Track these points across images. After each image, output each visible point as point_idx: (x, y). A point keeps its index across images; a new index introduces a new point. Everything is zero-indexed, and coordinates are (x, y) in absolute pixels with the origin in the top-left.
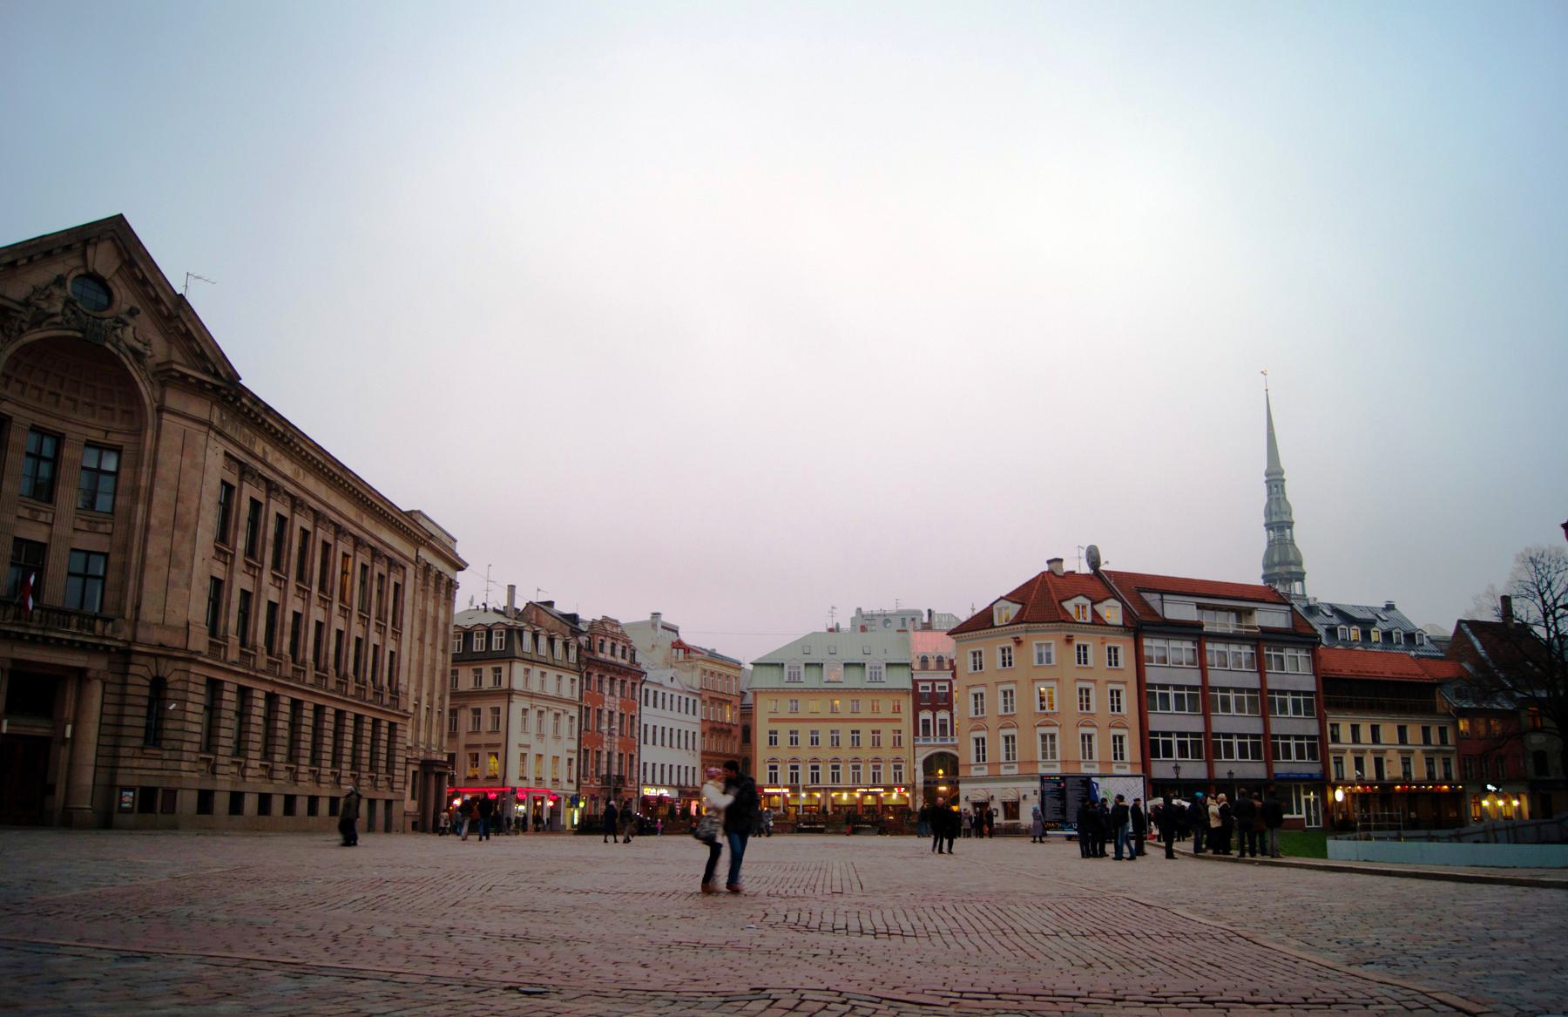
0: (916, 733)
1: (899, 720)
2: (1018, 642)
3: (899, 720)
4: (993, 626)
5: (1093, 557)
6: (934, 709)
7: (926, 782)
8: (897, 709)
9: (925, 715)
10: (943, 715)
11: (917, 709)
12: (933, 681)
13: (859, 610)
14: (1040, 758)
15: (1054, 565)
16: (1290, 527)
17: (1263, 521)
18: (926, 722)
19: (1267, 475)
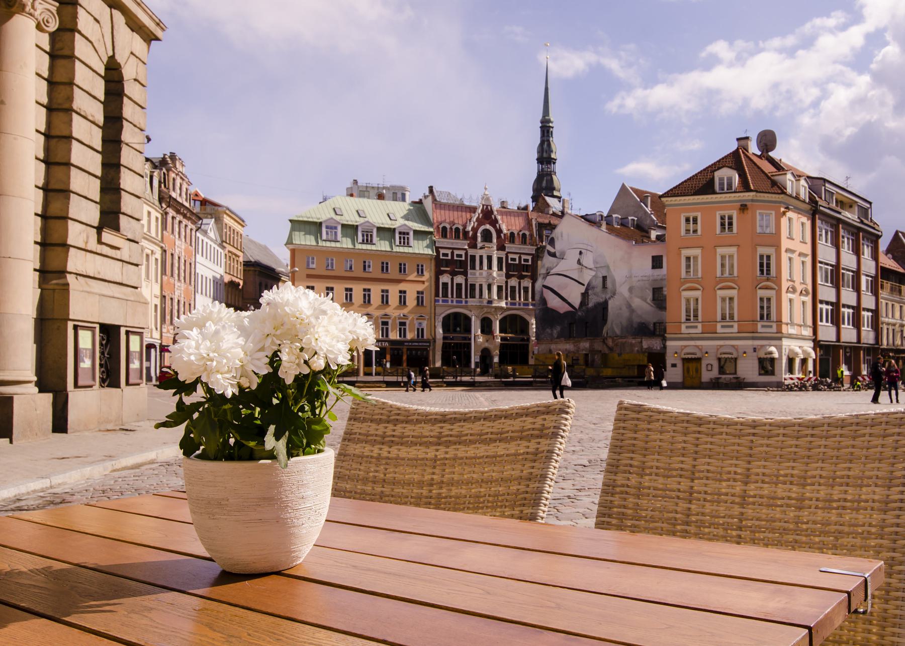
0: (437, 295)
2: (743, 208)
4: (714, 193)
5: (768, 141)
6: (453, 274)
7: (444, 338)
9: (445, 279)
10: (459, 279)
11: (438, 273)
12: (453, 249)
13: (356, 182)
14: (759, 319)
15: (743, 142)
16: (554, 163)
17: (536, 156)
18: (445, 285)
19: (542, 122)
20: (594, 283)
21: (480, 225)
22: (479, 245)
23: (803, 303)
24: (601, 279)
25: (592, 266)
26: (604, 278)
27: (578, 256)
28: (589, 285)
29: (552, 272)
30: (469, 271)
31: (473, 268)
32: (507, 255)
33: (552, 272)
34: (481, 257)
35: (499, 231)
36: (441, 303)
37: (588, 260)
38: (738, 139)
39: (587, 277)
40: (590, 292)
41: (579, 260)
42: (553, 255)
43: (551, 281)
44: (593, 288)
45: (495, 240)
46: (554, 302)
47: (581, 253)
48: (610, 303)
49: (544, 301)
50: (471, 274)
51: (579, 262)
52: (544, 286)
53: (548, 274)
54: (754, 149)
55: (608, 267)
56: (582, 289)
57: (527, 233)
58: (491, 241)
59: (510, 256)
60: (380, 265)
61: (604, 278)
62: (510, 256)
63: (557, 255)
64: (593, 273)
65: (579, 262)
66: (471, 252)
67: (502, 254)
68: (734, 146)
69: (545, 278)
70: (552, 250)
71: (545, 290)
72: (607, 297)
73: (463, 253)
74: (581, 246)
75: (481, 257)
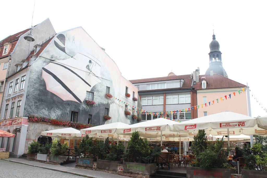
20: (99, 88)
25: (99, 76)
27: (88, 63)
33: (57, 61)
37: (95, 69)
39: (93, 82)
41: (88, 66)
43: (51, 67)
44: (98, 91)
46: (53, 87)
47: (90, 62)
48: (111, 106)
49: (43, 84)
51: (88, 67)
52: (43, 69)
53: (52, 61)
55: (112, 82)
56: (89, 89)
61: (108, 88)
64: (100, 81)
65: (88, 67)
71: (44, 73)
72: (110, 102)
74: (92, 58)
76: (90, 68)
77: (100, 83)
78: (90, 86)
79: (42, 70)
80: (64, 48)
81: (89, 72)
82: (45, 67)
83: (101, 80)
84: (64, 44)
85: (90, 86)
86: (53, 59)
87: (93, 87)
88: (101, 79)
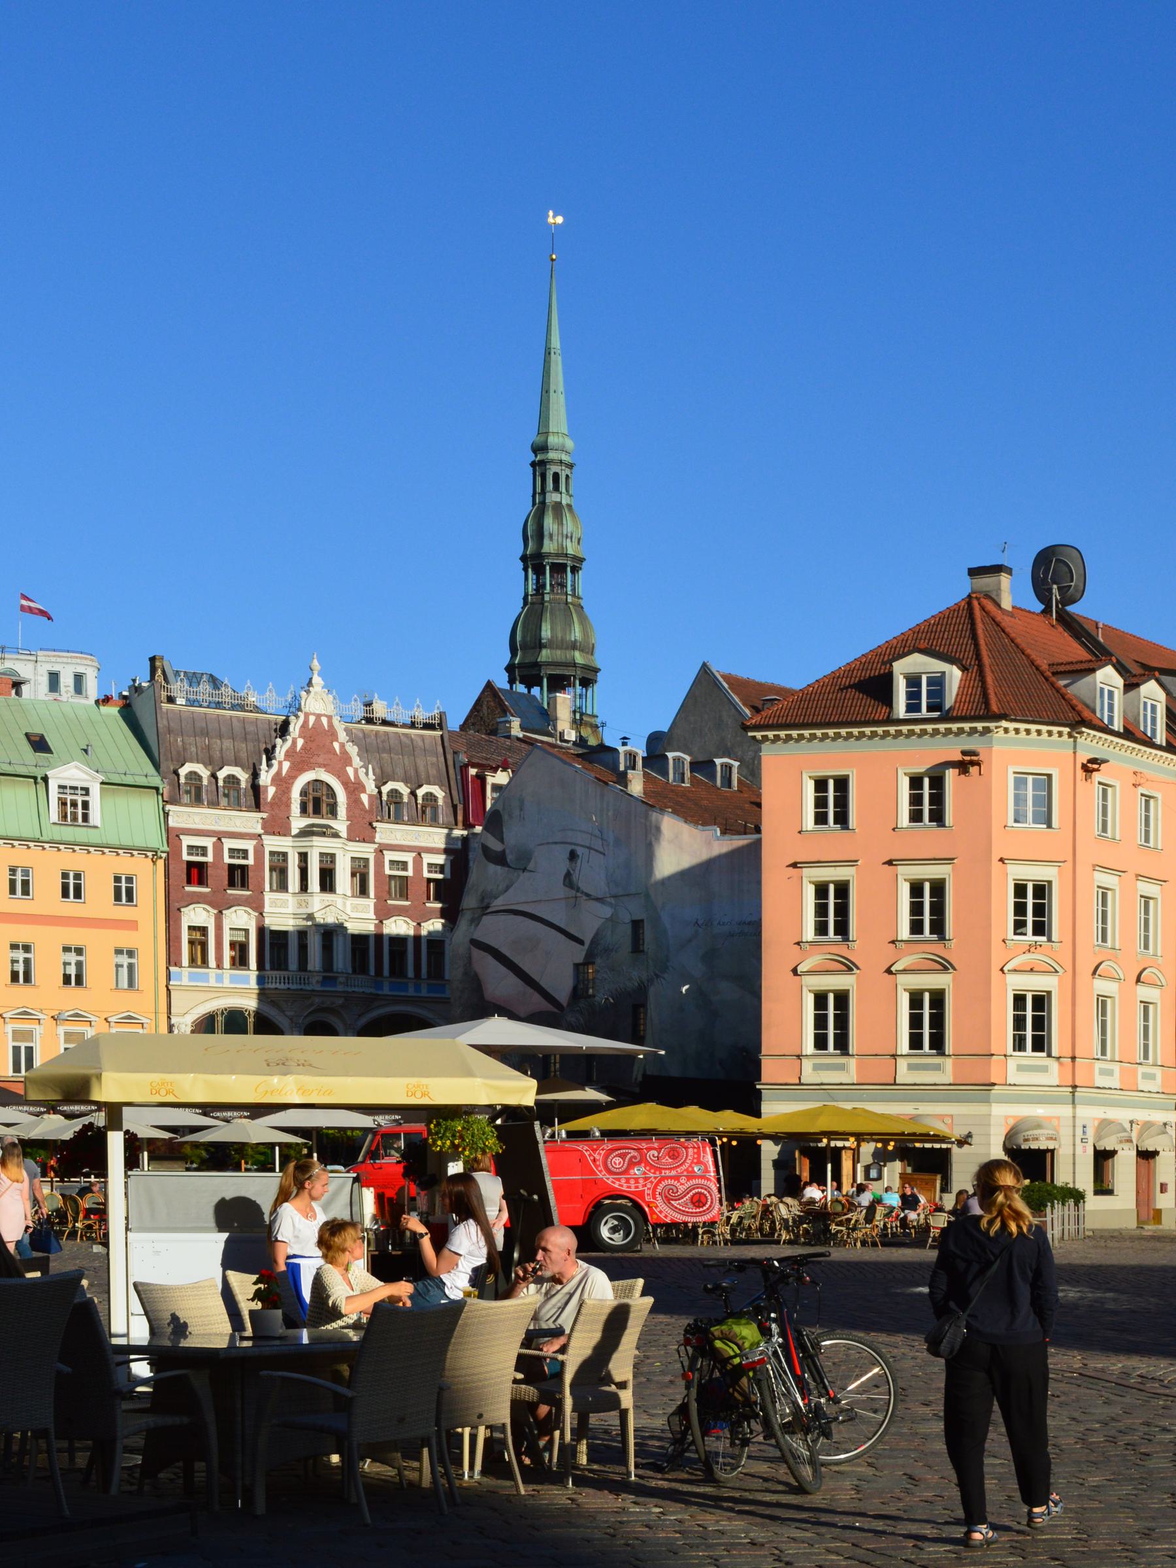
1: (132, 925)
3: (132, 925)
6: (221, 906)
8: (124, 892)
9: (196, 915)
10: (240, 919)
15: (985, 582)
21: (300, 766)
22: (298, 823)
23: (1146, 1005)
24: (628, 929)
26: (637, 925)
28: (594, 942)
29: (498, 903)
30: (269, 897)
31: (283, 886)
32: (380, 852)
33: (498, 903)
34: (303, 857)
35: (354, 788)
36: (185, 981)
38: (974, 572)
39: (591, 920)
40: (598, 961)
41: (568, 875)
42: (499, 859)
44: (607, 951)
45: (342, 810)
47: (573, 856)
50: (274, 903)
53: (484, 909)
54: (1014, 593)
56: (578, 954)
57: (439, 793)
58: (333, 812)
59: (389, 856)
60: (7, 877)
62: (389, 856)
63: (510, 858)
64: (606, 911)
66: (273, 843)
67: (366, 850)
68: (959, 589)
69: (475, 921)
70: (494, 845)
71: (477, 953)
73: (249, 845)
75: (303, 857)
76: (575, 878)
77: (610, 919)
78: (581, 942)
79: (469, 949)
80: (504, 851)
81: (573, 893)
82: (475, 937)
83: (610, 904)
84: (502, 840)
85: (581, 942)
86: (485, 904)
87: (592, 942)
88: (613, 901)
